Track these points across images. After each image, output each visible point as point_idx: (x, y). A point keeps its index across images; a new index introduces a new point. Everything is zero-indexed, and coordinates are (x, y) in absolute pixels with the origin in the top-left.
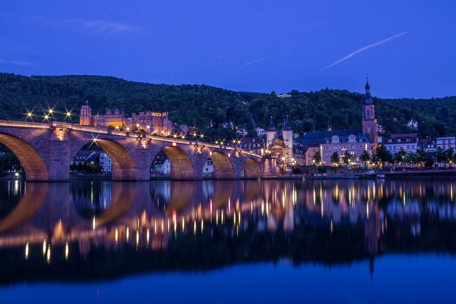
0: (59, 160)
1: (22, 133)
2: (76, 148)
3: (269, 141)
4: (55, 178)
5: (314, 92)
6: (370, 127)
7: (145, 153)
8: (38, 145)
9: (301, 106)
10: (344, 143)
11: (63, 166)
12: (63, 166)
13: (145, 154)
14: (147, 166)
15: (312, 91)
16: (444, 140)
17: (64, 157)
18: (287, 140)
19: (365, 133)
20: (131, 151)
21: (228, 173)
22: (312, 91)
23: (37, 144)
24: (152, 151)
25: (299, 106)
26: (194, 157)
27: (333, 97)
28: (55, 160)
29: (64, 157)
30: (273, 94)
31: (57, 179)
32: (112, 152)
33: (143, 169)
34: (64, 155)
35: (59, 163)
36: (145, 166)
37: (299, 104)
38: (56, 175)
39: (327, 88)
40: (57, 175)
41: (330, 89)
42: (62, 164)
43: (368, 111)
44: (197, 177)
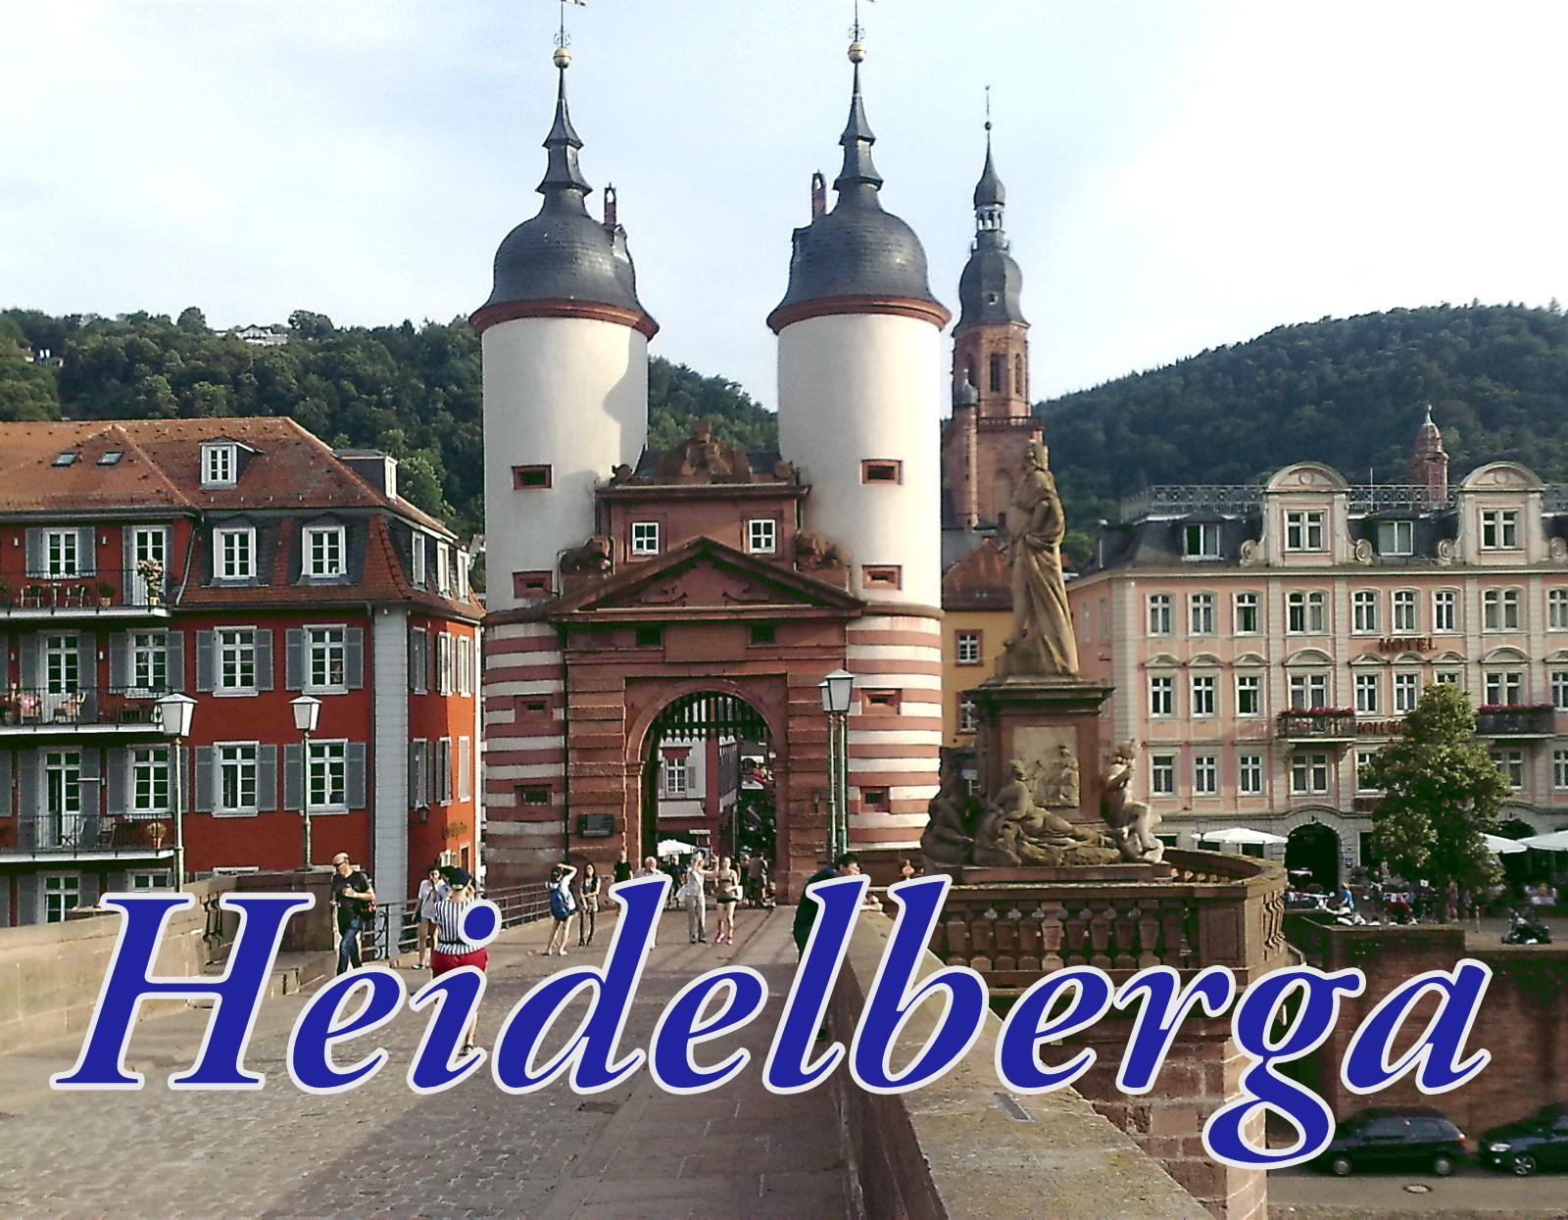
3: (534, 477)
5: (418, 327)
9: (359, 382)
10: (1405, 562)
15: (407, 323)
18: (883, 472)
19: (975, 522)
22: (407, 323)
30: (192, 318)
37: (344, 376)
43: (997, 361)
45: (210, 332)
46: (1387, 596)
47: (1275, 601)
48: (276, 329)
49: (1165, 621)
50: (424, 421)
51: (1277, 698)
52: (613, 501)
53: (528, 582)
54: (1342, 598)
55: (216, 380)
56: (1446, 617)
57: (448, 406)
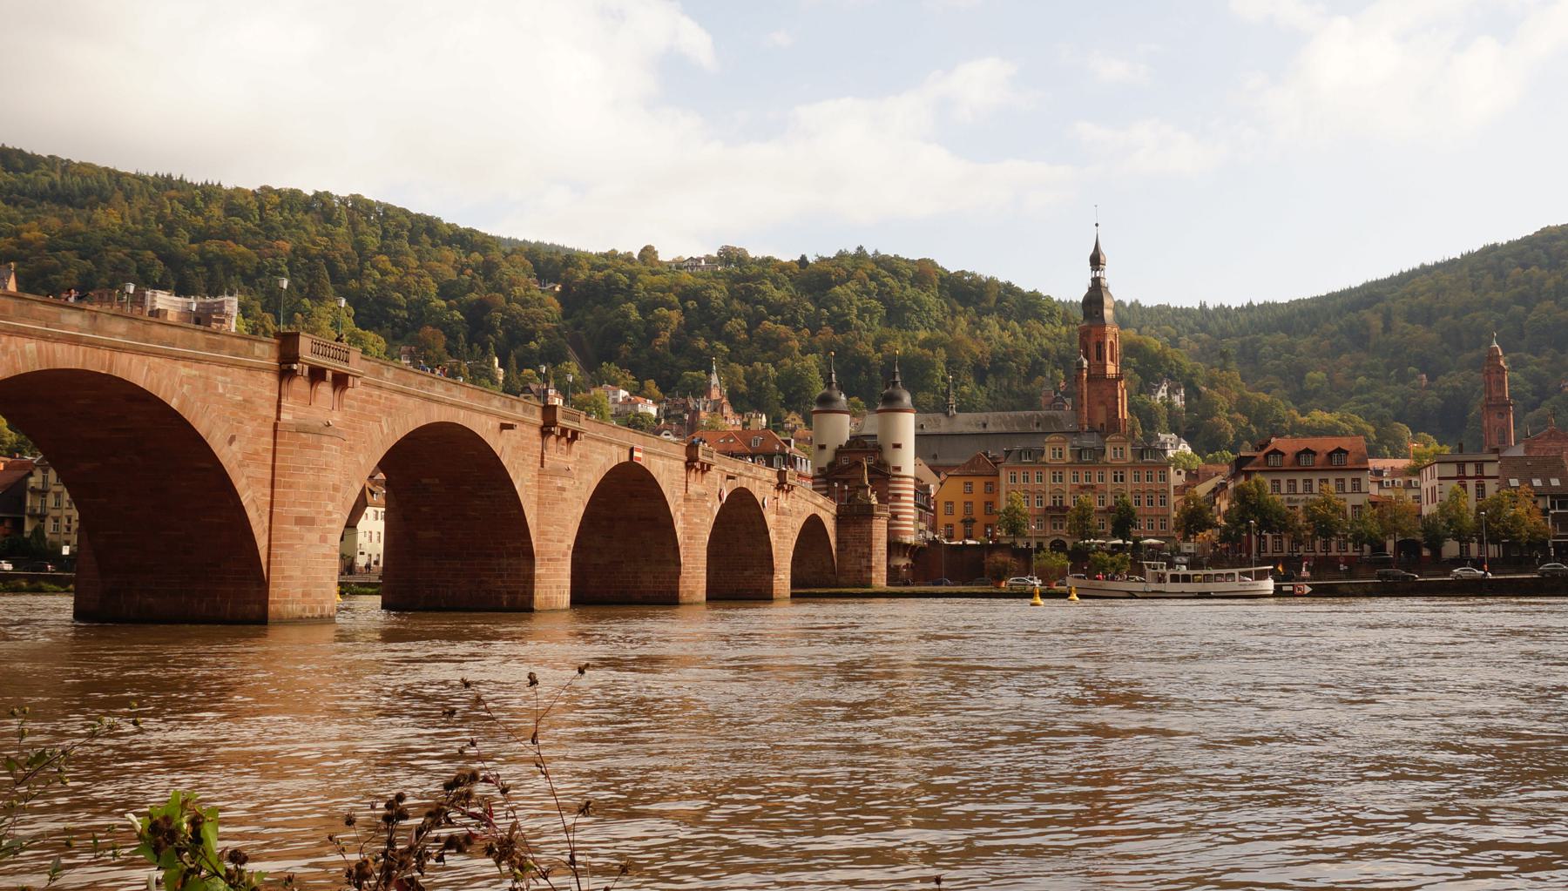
1: (181, 385)
2: (362, 461)
3: (822, 447)
5: (811, 259)
6: (1102, 403)
7: (562, 489)
8: (235, 447)
13: (565, 495)
15: (803, 258)
16: (1461, 465)
18: (898, 446)
21: (747, 573)
22: (803, 258)
23: (232, 440)
25: (762, 308)
27: (885, 285)
28: (300, 521)
29: (330, 508)
30: (648, 253)
32: (425, 481)
34: (332, 499)
35: (313, 537)
37: (759, 302)
38: (300, 590)
39: (860, 248)
40: (304, 594)
41: (870, 252)
42: (323, 539)
45: (661, 263)
46: (1082, 474)
47: (1048, 475)
48: (708, 259)
49: (1026, 479)
50: (813, 334)
51: (1048, 502)
52: (840, 451)
53: (820, 470)
54: (1068, 475)
55: (670, 308)
56: (1101, 479)
57: (830, 321)
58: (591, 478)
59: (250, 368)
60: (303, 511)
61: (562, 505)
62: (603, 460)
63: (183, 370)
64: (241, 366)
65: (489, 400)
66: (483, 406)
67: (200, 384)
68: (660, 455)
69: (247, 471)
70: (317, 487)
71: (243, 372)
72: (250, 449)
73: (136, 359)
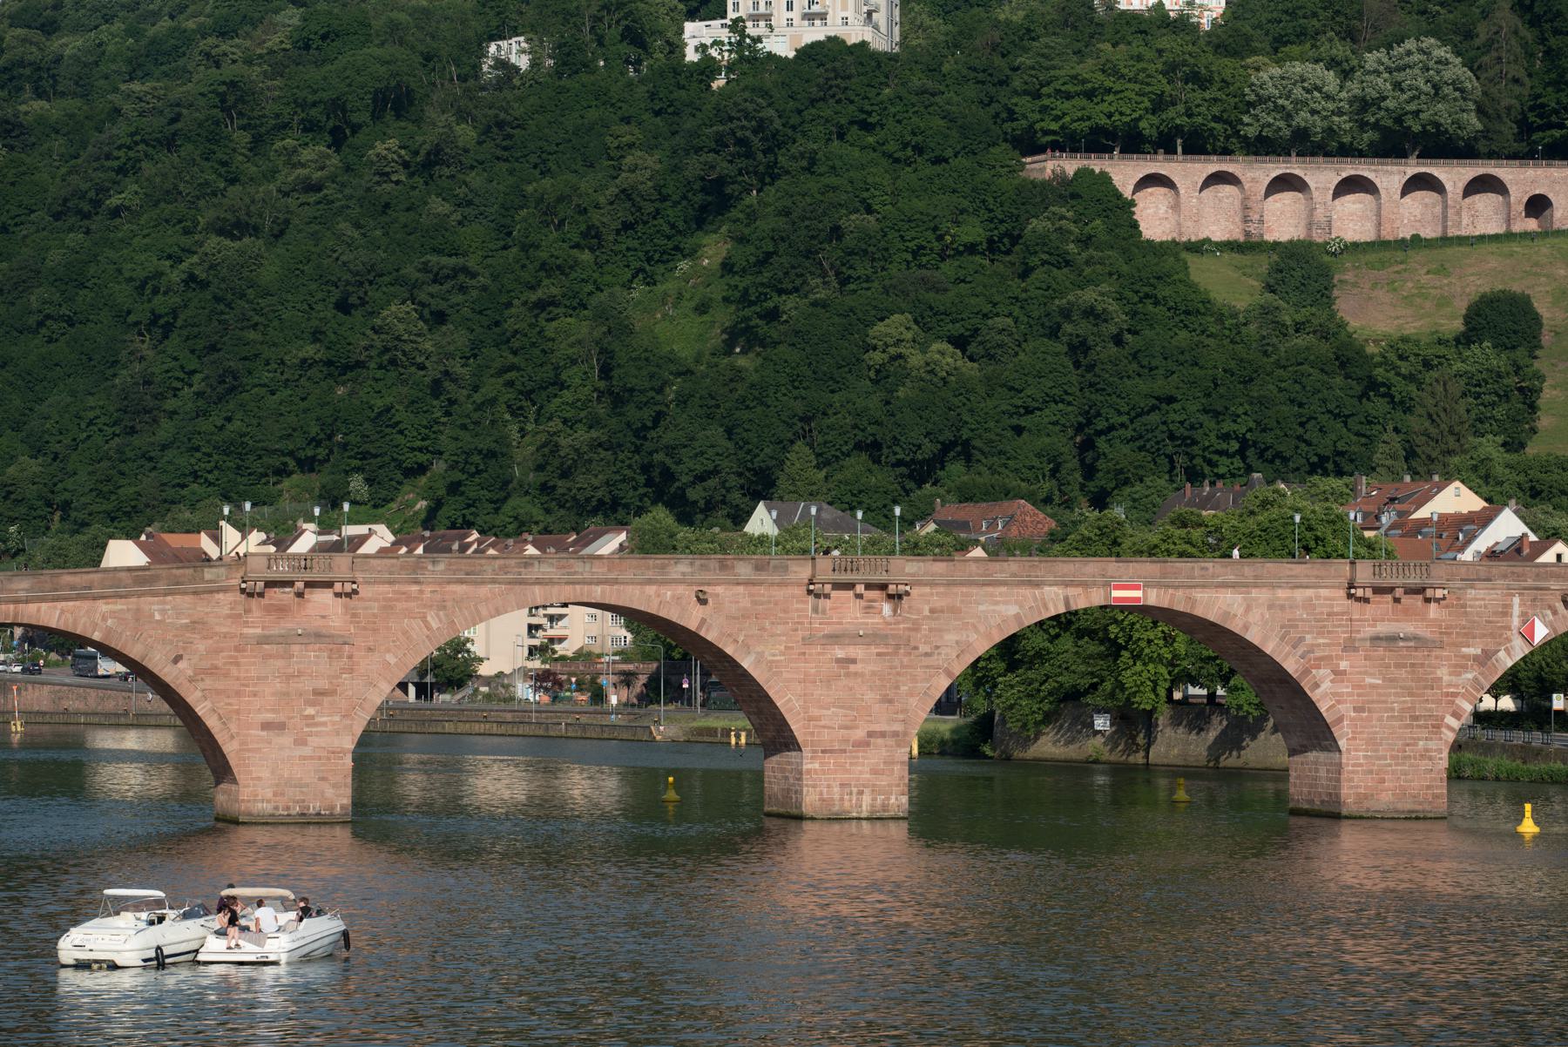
0: (280, 727)
1: (104, 619)
4: (263, 807)
7: (854, 661)
8: (181, 665)
11: (307, 751)
12: (307, 751)
14: (883, 734)
17: (310, 711)
20: (761, 654)
23: (177, 659)
24: (923, 648)
26: (1343, 665)
28: (266, 726)
29: (310, 711)
31: (276, 808)
33: (844, 751)
35: (286, 740)
36: (860, 734)
40: (275, 794)
44: (1366, 797)
58: (973, 637)
59: (195, 593)
60: (269, 717)
61: (844, 681)
62: (1012, 610)
63: (103, 607)
64: (185, 593)
65: (663, 567)
66: (650, 575)
67: (129, 616)
68: (1233, 586)
69: (201, 685)
70: (287, 694)
71: (188, 598)
72: (206, 664)
73: (44, 606)
